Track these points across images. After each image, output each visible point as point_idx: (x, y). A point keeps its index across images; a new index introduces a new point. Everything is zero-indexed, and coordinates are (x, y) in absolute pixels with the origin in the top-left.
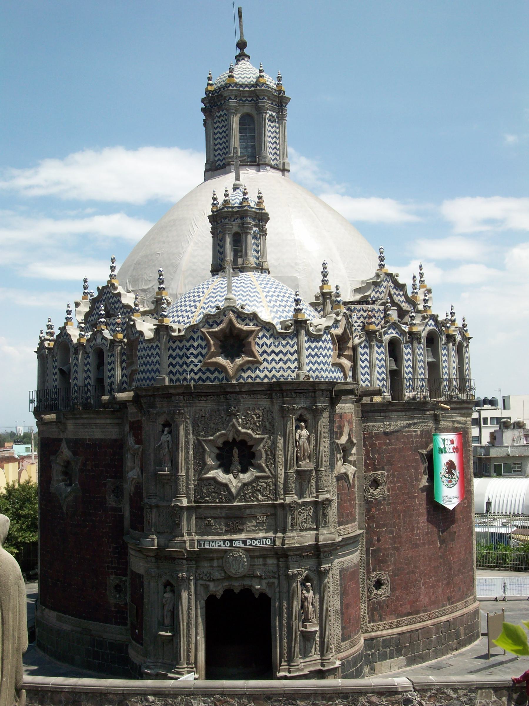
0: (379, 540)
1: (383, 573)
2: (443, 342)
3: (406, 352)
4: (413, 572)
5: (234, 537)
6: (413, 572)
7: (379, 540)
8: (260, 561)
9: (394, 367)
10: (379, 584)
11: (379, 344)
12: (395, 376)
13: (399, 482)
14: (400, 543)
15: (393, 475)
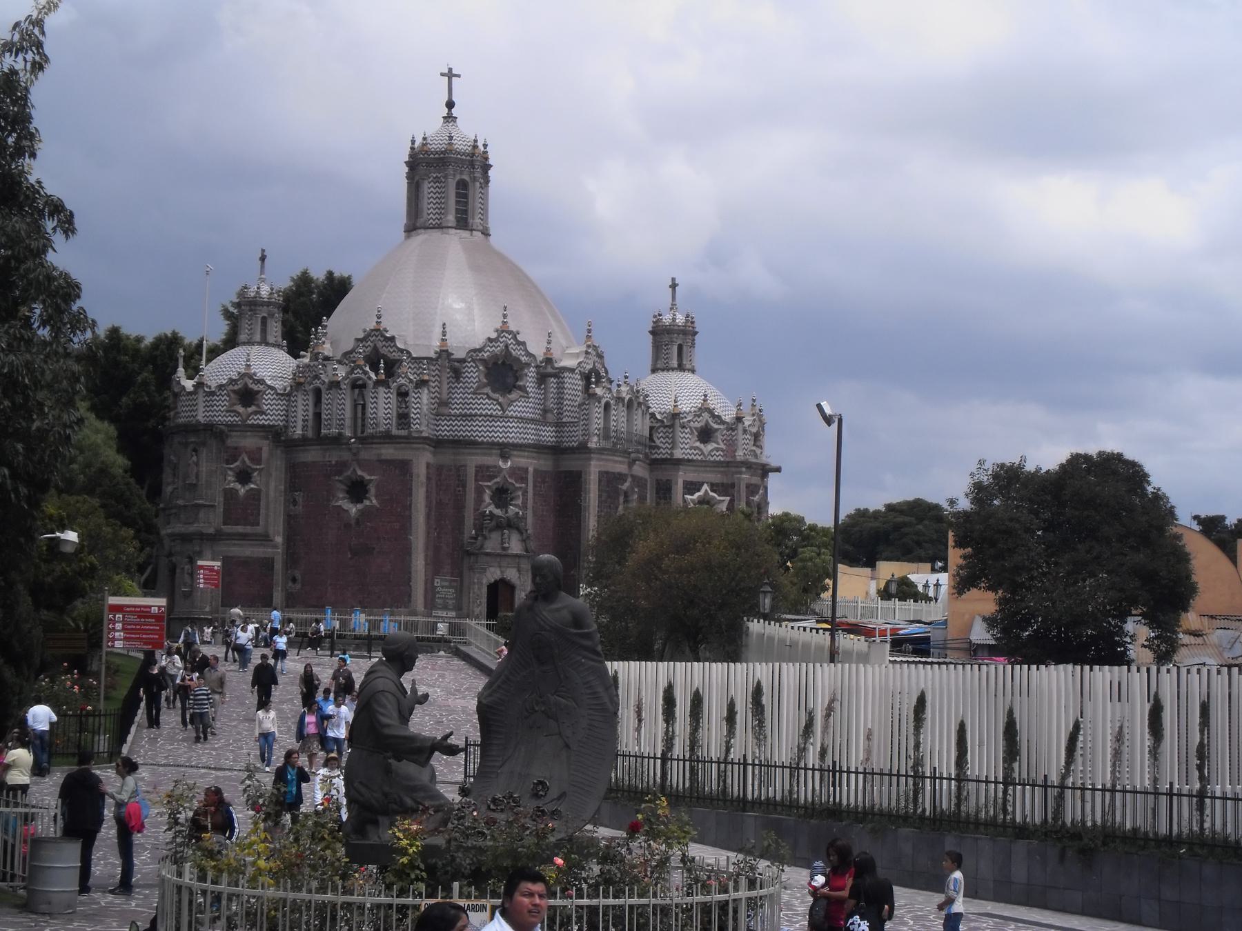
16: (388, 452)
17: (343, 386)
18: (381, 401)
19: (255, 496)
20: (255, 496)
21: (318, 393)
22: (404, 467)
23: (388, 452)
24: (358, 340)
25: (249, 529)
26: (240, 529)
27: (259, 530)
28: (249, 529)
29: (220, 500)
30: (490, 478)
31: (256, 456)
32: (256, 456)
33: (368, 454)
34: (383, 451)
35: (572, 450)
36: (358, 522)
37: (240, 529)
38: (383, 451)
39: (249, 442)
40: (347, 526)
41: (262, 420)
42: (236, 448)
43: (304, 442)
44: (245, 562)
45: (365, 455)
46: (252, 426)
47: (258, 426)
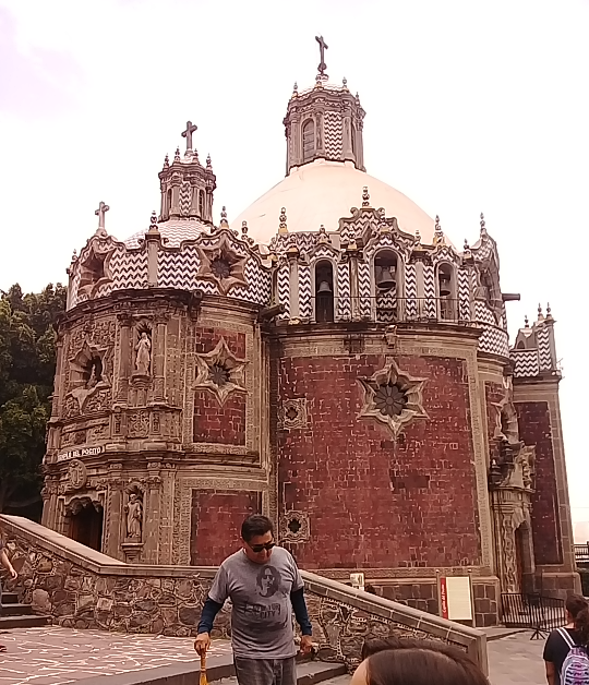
0: (295, 474)
1: (300, 512)
2: (407, 261)
3: (339, 273)
4: (346, 516)
5: (79, 447)
6: (346, 516)
7: (295, 474)
8: (94, 472)
9: (324, 287)
10: (295, 526)
11: (303, 268)
12: (324, 300)
13: (323, 411)
14: (325, 479)
15: (317, 403)
16: (436, 346)
17: (365, 258)
18: (420, 280)
19: (238, 402)
20: (238, 402)
21: (324, 271)
22: (455, 366)
23: (436, 346)
24: (344, 220)
25: (231, 448)
26: (219, 448)
27: (243, 450)
28: (231, 448)
29: (188, 404)
30: (500, 398)
31: (237, 344)
32: (237, 344)
33: (414, 345)
34: (428, 345)
35: (534, 380)
36: (401, 439)
37: (219, 448)
38: (428, 345)
39: (230, 323)
40: (386, 445)
41: (245, 295)
42: (211, 331)
43: (306, 328)
44: (227, 499)
45: (402, 349)
46: (233, 301)
47: (242, 303)
